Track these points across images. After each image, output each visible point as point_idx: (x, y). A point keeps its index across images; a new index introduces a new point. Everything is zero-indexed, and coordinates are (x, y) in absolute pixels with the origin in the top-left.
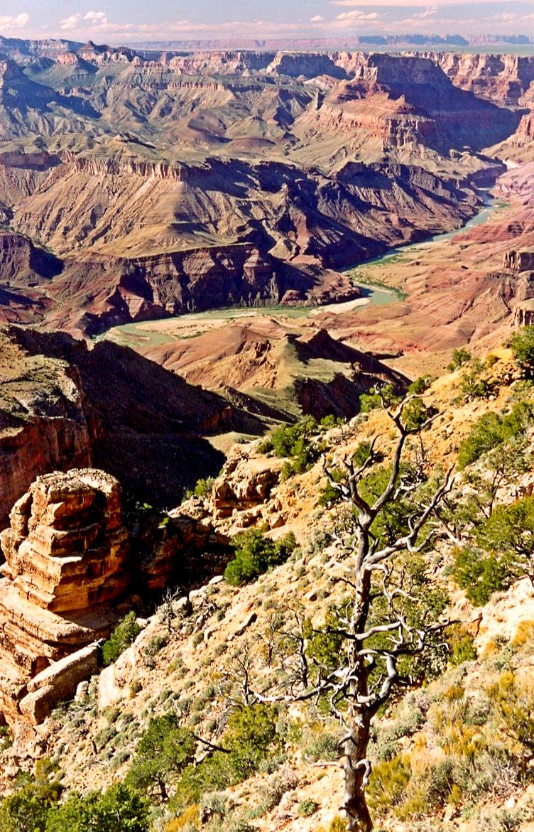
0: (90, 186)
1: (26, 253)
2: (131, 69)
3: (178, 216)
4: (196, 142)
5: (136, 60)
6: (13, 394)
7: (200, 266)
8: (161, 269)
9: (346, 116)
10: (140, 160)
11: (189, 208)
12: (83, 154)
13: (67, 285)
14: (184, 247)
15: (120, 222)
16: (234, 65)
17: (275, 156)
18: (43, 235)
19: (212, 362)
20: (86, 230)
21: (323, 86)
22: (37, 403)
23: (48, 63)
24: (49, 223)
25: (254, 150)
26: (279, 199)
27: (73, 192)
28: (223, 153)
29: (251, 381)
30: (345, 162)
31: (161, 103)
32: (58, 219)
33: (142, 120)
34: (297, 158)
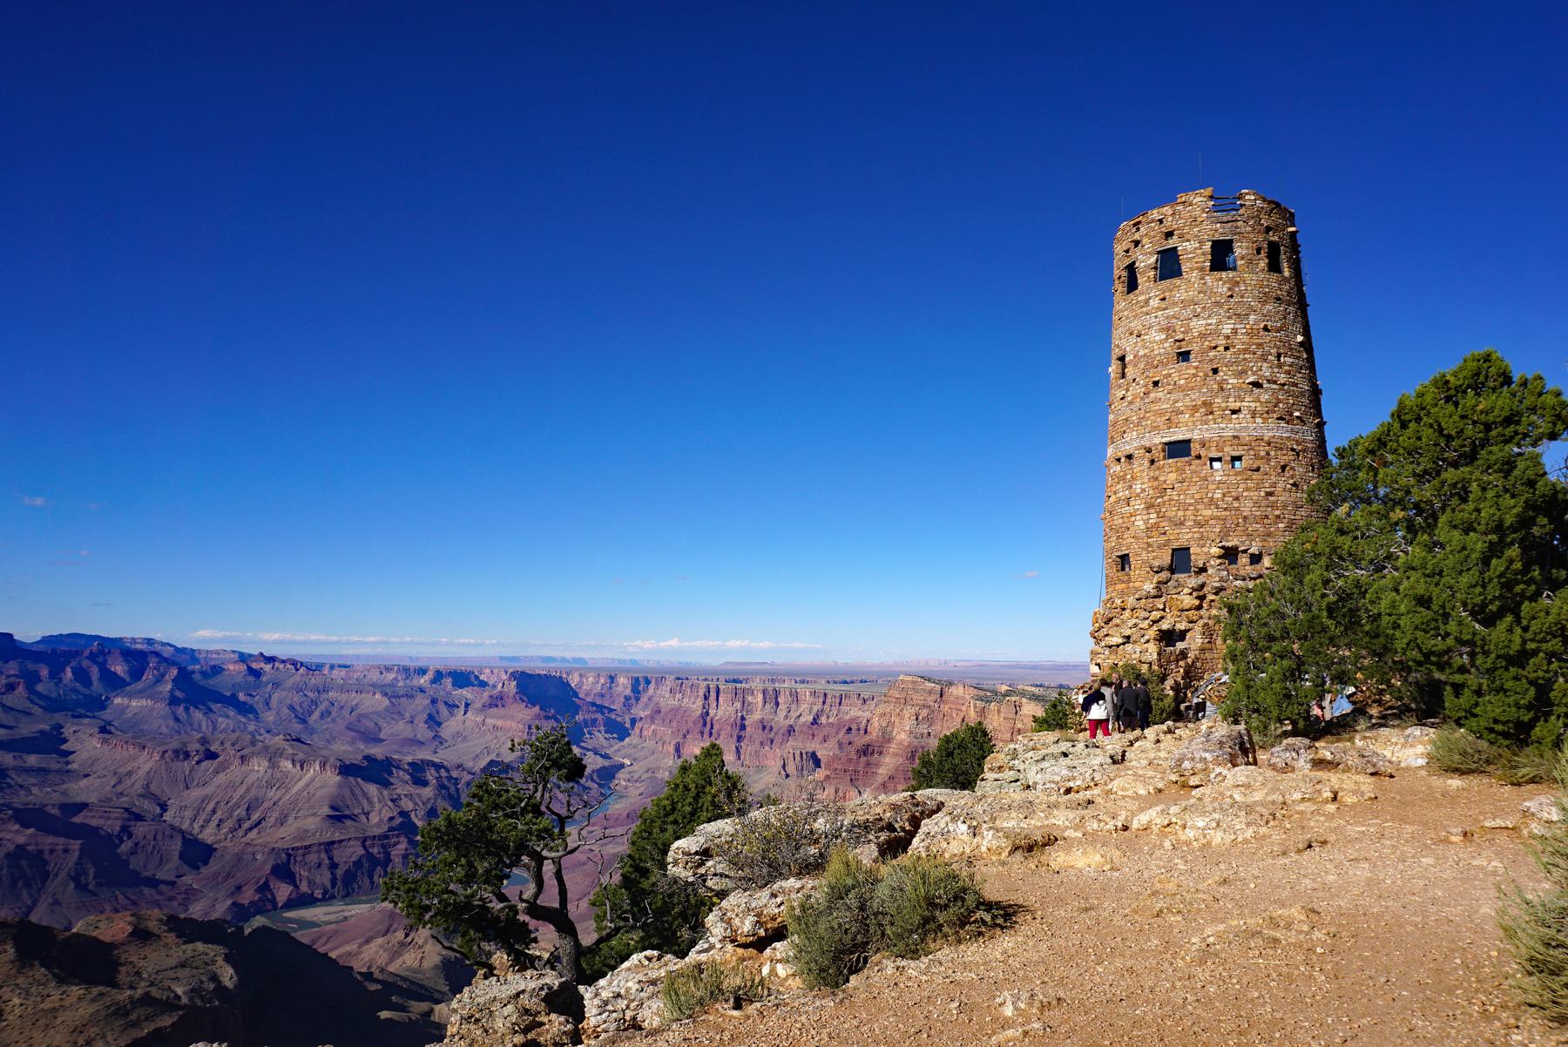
0: (249, 781)
1: (177, 845)
2: (297, 678)
3: (333, 808)
4: (353, 742)
5: (302, 670)
6: (167, 983)
7: (350, 853)
8: (313, 858)
9: (489, 721)
10: (301, 756)
11: (343, 800)
12: (246, 752)
13: (216, 875)
14: (337, 836)
15: (275, 815)
16: (390, 676)
17: (424, 754)
18: (196, 826)
19: (360, 946)
20: (240, 821)
21: (469, 696)
22: (192, 990)
23: (217, 670)
24: (203, 816)
25: (406, 750)
26: (428, 792)
27: (232, 786)
28: (378, 751)
29: (399, 961)
30: (488, 759)
31: (322, 707)
32: (214, 811)
33: (304, 721)
34: (444, 756)
